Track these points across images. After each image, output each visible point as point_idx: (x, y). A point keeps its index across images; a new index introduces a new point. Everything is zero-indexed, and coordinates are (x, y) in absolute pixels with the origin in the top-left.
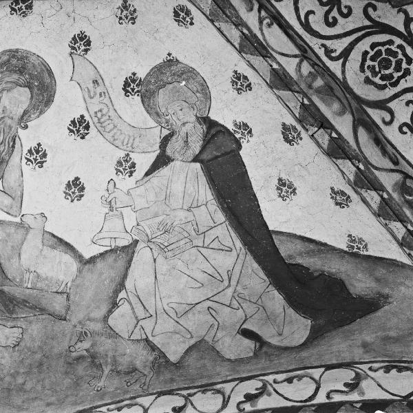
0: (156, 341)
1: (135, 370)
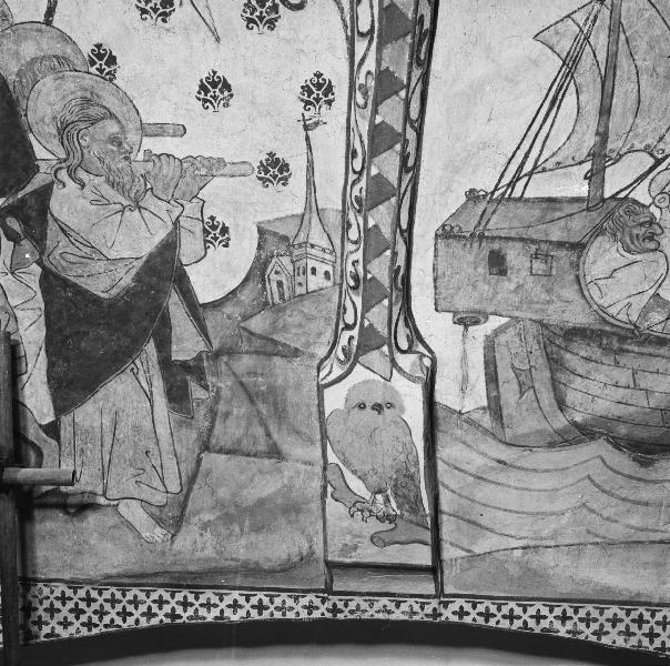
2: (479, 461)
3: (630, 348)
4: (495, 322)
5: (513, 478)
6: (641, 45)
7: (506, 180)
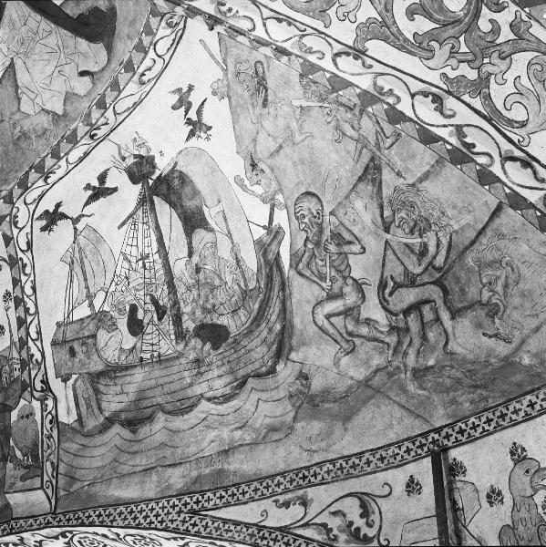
0: (48, 107)
1: (46, 130)
2: (75, 446)
3: (118, 374)
4: (74, 377)
5: (87, 453)
6: (88, 253)
7: (66, 315)
